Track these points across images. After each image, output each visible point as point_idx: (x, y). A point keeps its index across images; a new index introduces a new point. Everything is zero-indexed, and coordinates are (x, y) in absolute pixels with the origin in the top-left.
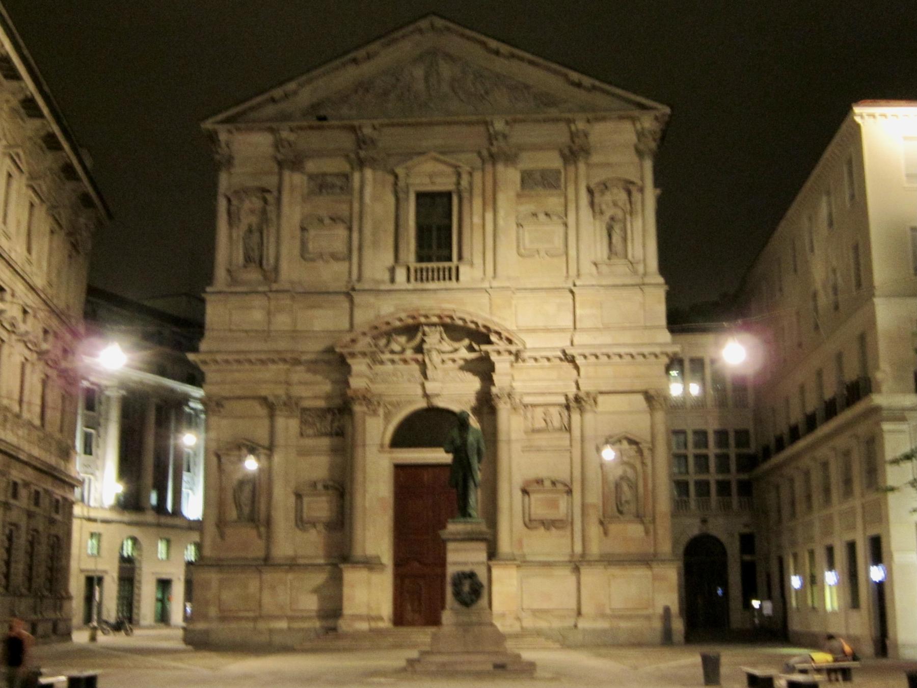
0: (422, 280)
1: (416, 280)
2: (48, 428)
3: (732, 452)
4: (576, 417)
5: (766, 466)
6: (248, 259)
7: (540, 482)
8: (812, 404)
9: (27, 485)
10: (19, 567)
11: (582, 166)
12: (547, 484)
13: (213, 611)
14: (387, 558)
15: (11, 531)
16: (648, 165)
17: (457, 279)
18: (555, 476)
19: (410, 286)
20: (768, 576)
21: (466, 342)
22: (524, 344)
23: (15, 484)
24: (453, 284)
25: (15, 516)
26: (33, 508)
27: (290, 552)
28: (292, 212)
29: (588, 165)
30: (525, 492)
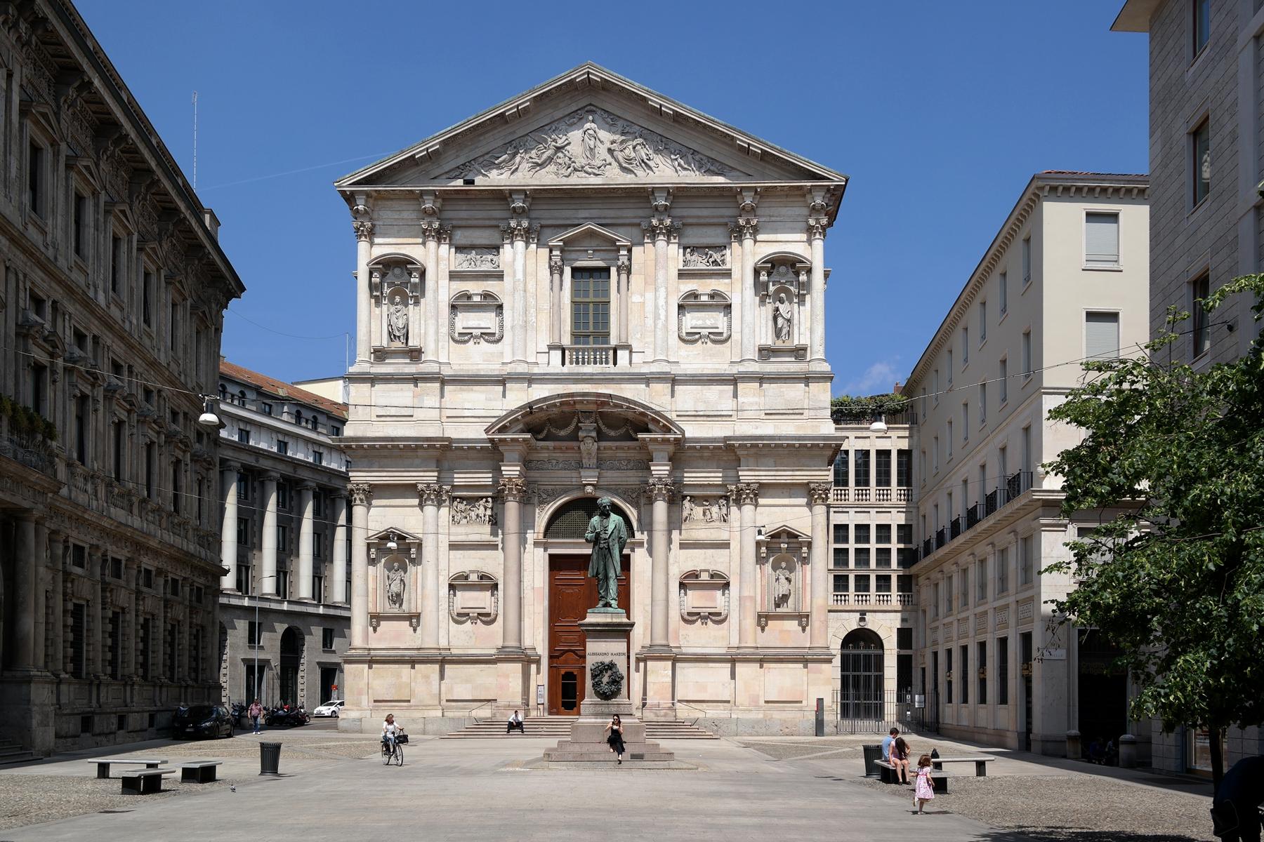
0: (577, 363)
1: (571, 363)
2: (184, 514)
3: (894, 546)
4: (734, 509)
5: (925, 562)
6: (392, 336)
7: (694, 575)
8: (975, 497)
9: (160, 572)
10: (159, 656)
11: (748, 243)
12: (705, 577)
13: (365, 701)
14: (542, 649)
15: (146, 620)
16: (818, 244)
17: (615, 364)
18: (711, 568)
19: (566, 369)
20: (924, 669)
21: (622, 431)
22: (683, 432)
23: (148, 572)
24: (610, 368)
25: (149, 605)
26: (169, 596)
27: (443, 643)
28: (440, 290)
29: (755, 241)
30: (682, 586)
